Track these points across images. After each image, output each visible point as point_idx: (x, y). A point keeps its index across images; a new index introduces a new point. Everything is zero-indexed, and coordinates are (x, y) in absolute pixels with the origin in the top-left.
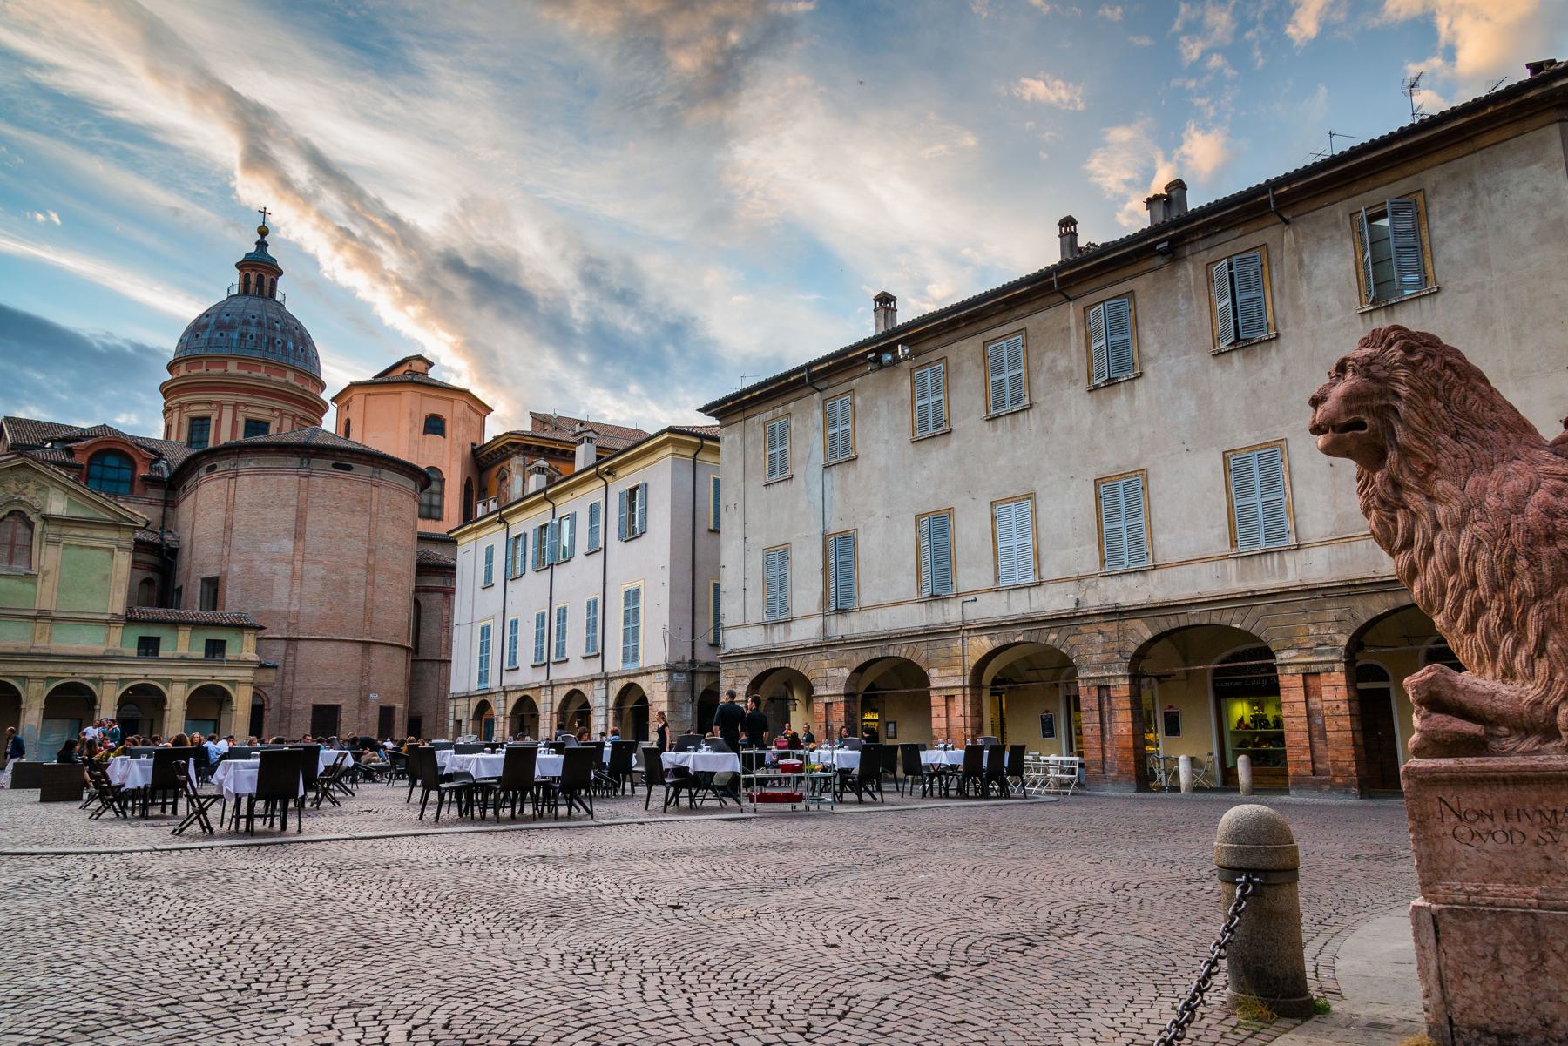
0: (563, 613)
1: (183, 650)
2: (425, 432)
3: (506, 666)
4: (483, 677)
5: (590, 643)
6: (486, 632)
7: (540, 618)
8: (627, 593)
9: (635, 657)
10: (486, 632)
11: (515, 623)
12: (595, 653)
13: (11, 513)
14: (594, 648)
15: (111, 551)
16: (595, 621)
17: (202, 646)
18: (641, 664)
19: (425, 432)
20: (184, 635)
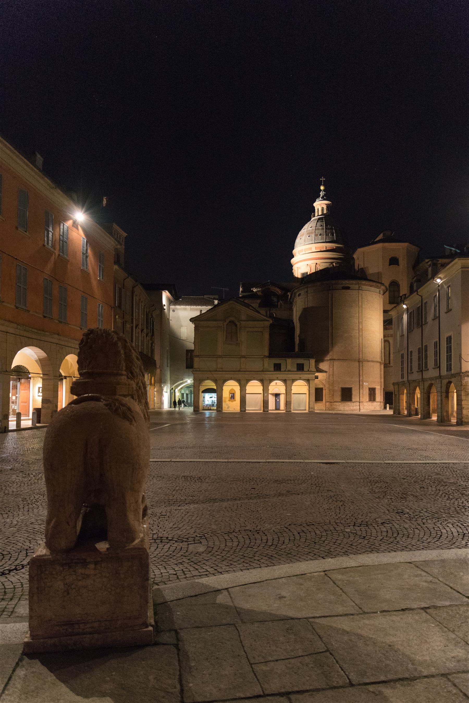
0: (426, 346)
1: (289, 367)
2: (390, 265)
3: (409, 371)
4: (402, 377)
5: (436, 361)
6: (402, 356)
7: (419, 349)
8: (447, 338)
9: (451, 369)
10: (402, 356)
11: (411, 352)
12: (438, 366)
13: (230, 322)
14: (437, 365)
15: (262, 332)
16: (437, 350)
17: (296, 366)
18: (453, 372)
19: (390, 265)
20: (289, 361)
